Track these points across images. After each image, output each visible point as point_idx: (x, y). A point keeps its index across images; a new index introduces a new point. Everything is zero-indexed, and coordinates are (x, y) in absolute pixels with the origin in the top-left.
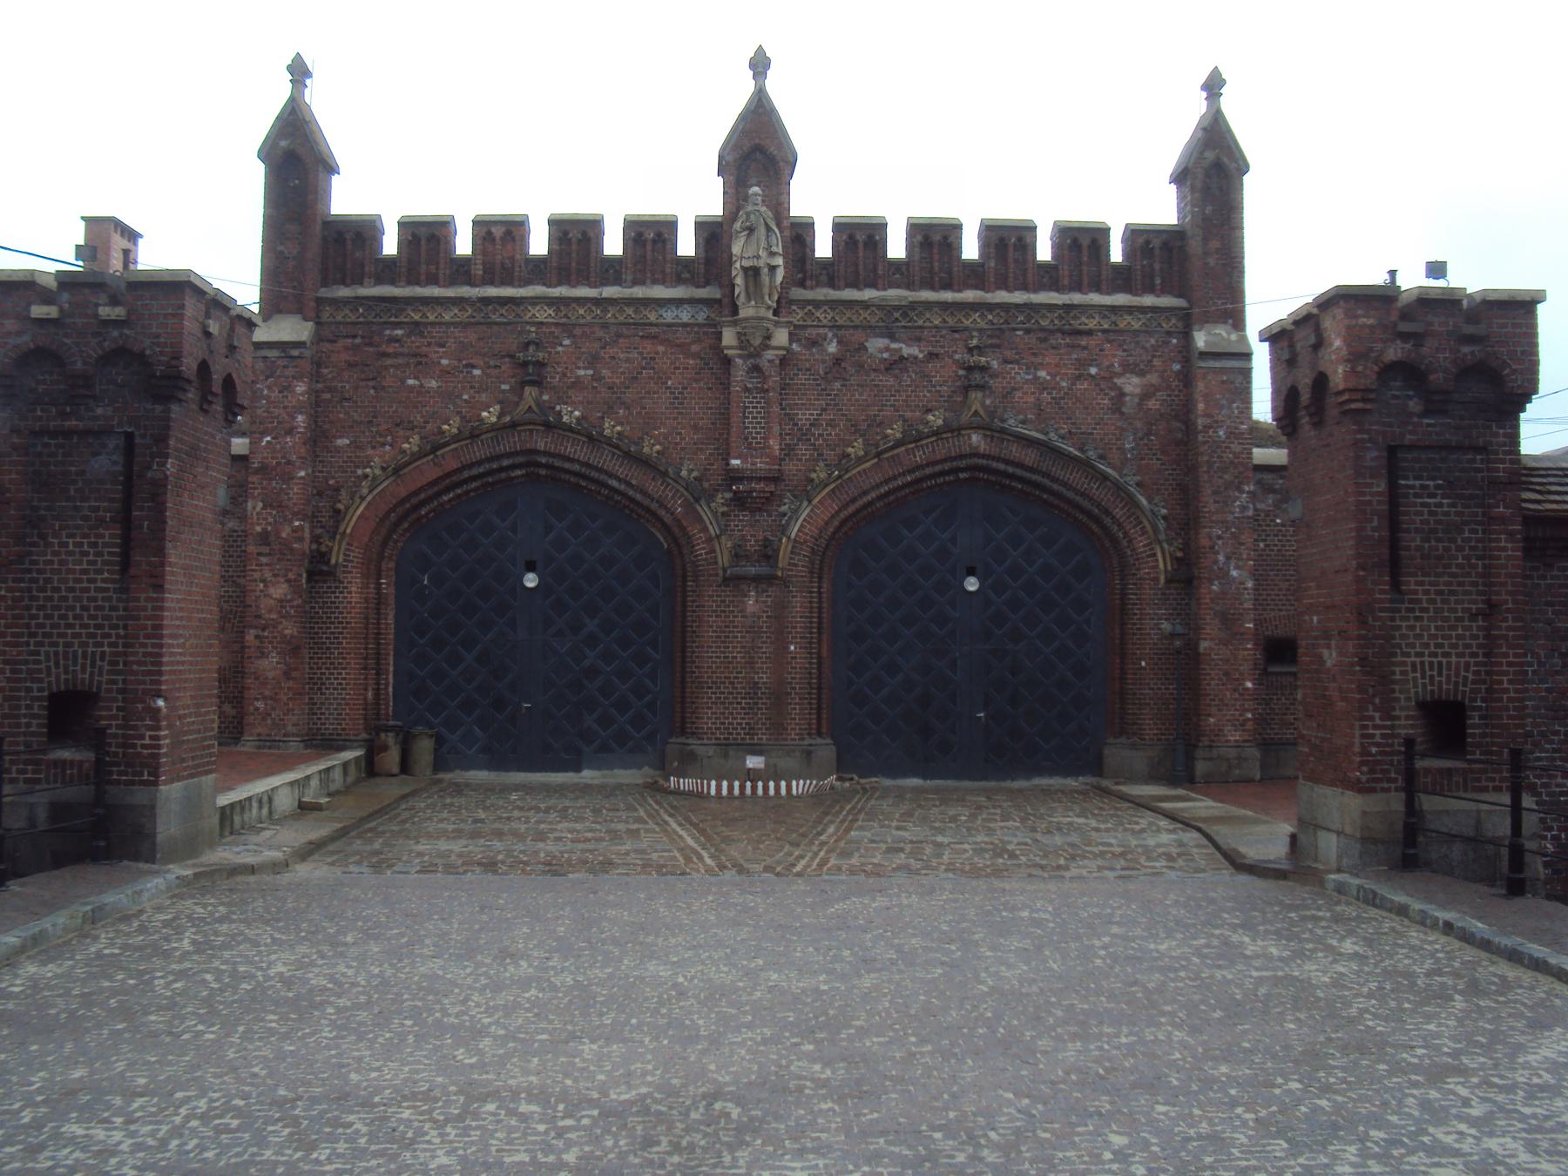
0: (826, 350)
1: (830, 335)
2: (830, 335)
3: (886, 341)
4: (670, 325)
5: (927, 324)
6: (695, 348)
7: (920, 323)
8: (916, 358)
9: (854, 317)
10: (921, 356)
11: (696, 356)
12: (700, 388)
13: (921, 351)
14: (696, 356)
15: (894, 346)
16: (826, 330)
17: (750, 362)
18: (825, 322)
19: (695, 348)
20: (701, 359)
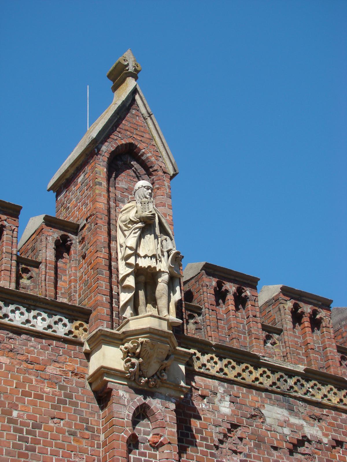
0: (217, 410)
1: (221, 390)
2: (221, 390)
3: (285, 413)
4: (18, 331)
5: (325, 401)
6: (52, 370)
7: (318, 398)
8: (320, 442)
9: (245, 375)
10: (325, 440)
11: (52, 381)
12: (60, 431)
13: (326, 435)
14: (52, 381)
15: (294, 420)
16: (216, 382)
17: (139, 399)
18: (213, 372)
19: (52, 370)
20: (62, 388)
